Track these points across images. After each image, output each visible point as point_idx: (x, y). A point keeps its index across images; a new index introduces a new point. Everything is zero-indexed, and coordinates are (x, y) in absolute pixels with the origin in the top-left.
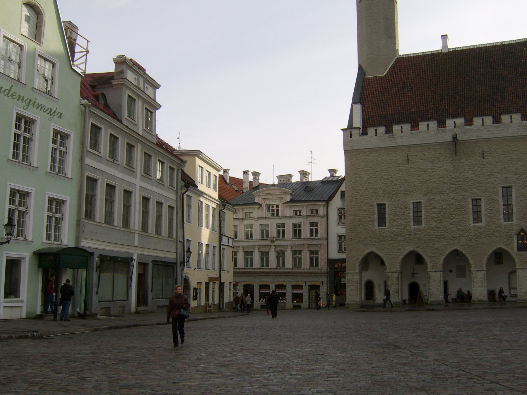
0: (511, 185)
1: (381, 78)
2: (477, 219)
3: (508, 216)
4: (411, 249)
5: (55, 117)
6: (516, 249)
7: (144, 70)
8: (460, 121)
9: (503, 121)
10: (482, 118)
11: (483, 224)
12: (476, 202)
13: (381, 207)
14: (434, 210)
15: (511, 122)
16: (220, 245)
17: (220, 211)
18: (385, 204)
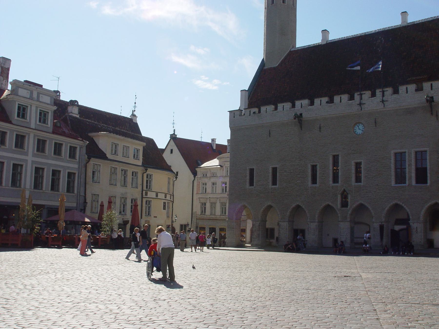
0: (338, 153)
1: (274, 68)
2: (314, 181)
3: (335, 179)
4: (269, 204)
6: (339, 205)
7: (41, 86)
8: (306, 102)
9: (335, 101)
10: (320, 99)
11: (317, 185)
12: (314, 168)
13: (252, 171)
14: (285, 173)
15: (341, 102)
16: (142, 197)
18: (253, 169)
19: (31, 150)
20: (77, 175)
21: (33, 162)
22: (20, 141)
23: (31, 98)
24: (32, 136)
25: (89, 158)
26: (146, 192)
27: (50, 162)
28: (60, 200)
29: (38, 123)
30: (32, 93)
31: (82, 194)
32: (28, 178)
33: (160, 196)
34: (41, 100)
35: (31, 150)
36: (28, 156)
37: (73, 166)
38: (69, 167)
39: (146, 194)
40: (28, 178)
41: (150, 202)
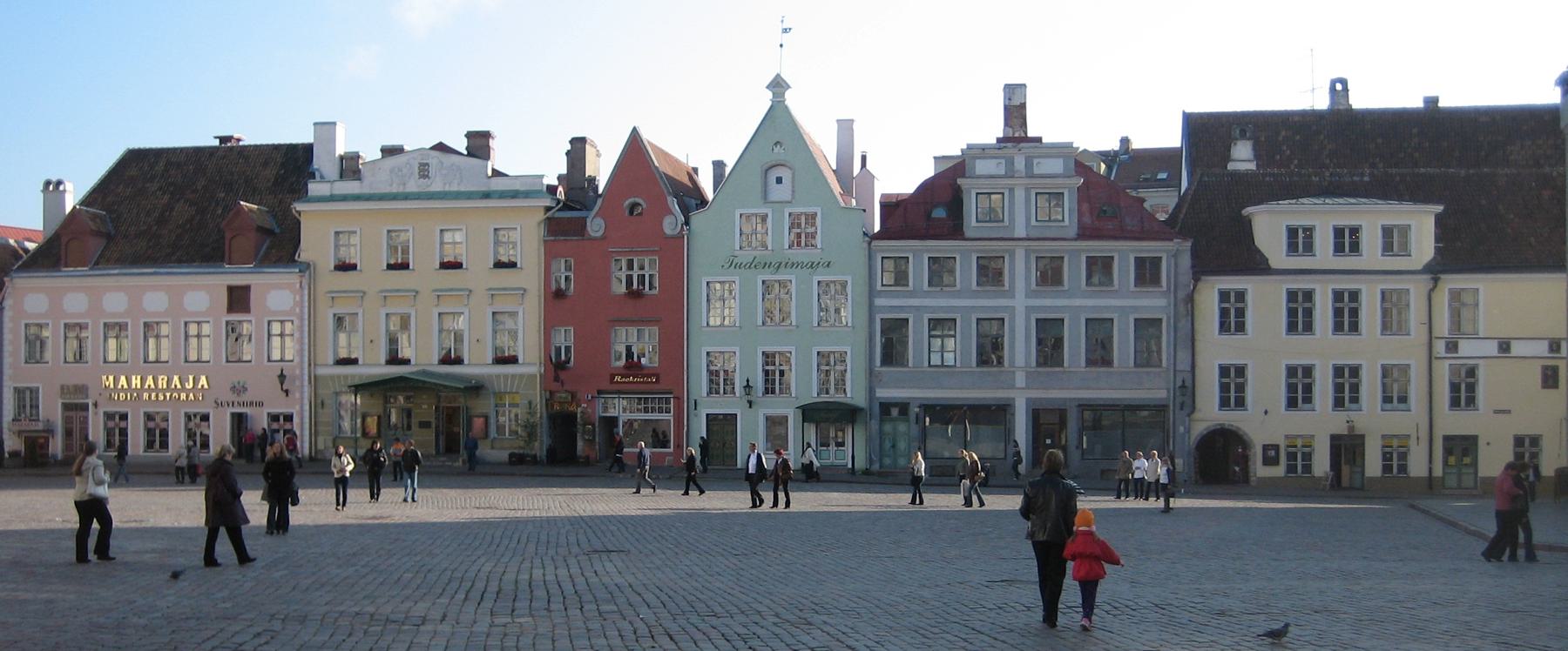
5: (820, 269)
17: (1432, 290)
19: (1020, 285)
20: (1164, 324)
21: (1029, 309)
22: (990, 273)
23: (1011, 174)
24: (1020, 255)
25: (1197, 280)
26: (1447, 344)
27: (1078, 302)
28: (1122, 384)
29: (1033, 222)
30: (1010, 162)
31: (1184, 365)
32: (1020, 347)
33: (1517, 349)
34: (1036, 171)
35: (1020, 285)
36: (1013, 297)
37: (1153, 303)
38: (1135, 309)
39: (1452, 347)
40: (1020, 347)
41: (1472, 372)
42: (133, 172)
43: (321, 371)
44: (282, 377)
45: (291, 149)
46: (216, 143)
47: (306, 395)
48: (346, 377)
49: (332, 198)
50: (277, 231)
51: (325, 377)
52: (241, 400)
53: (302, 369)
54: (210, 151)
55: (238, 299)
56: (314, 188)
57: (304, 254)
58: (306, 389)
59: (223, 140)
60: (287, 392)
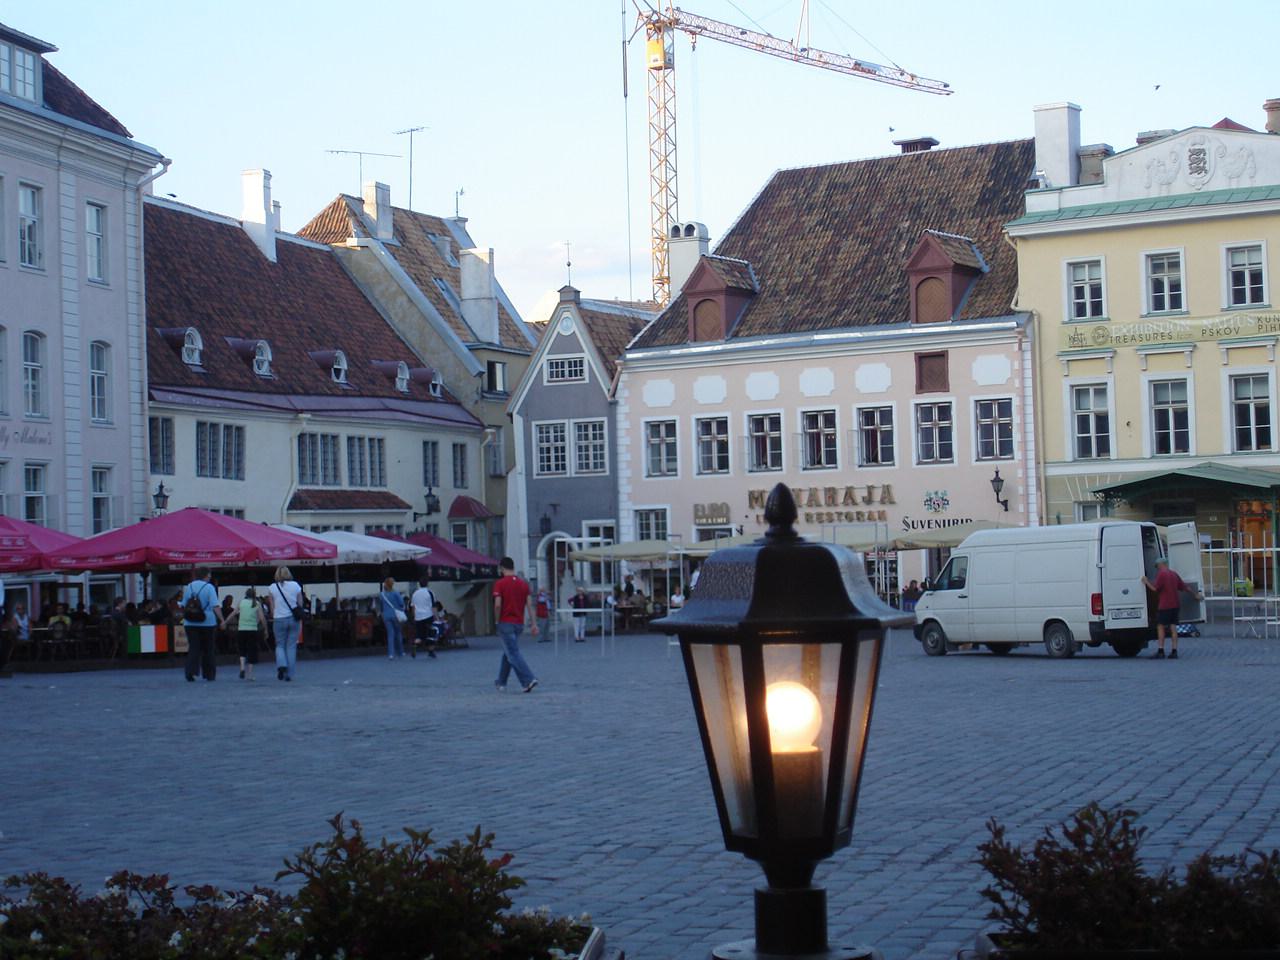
42: (784, 202)
43: (1052, 471)
44: (997, 482)
45: (1005, 149)
46: (898, 151)
47: (1034, 508)
48: (1092, 478)
49: (1060, 214)
50: (986, 269)
51: (1060, 478)
52: (940, 517)
53: (1026, 469)
54: (890, 164)
55: (931, 369)
56: (1034, 202)
57: (1024, 300)
58: (1033, 499)
59: (907, 146)
60: (1005, 503)
